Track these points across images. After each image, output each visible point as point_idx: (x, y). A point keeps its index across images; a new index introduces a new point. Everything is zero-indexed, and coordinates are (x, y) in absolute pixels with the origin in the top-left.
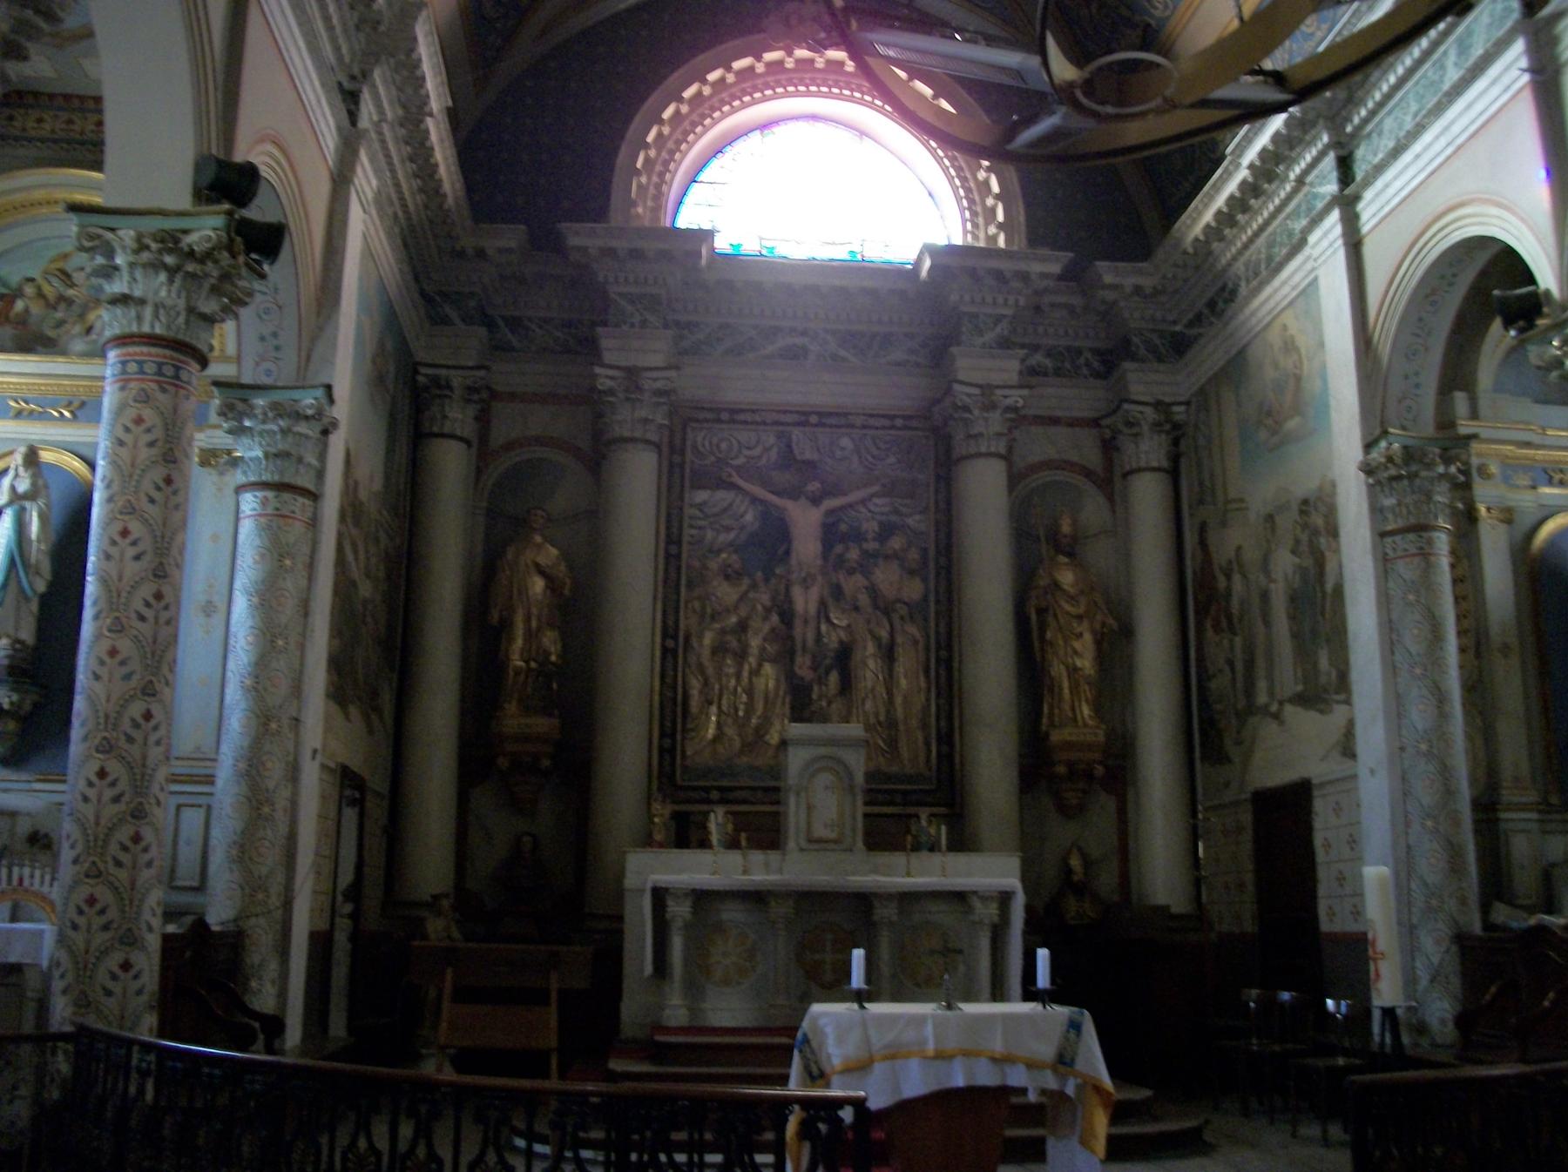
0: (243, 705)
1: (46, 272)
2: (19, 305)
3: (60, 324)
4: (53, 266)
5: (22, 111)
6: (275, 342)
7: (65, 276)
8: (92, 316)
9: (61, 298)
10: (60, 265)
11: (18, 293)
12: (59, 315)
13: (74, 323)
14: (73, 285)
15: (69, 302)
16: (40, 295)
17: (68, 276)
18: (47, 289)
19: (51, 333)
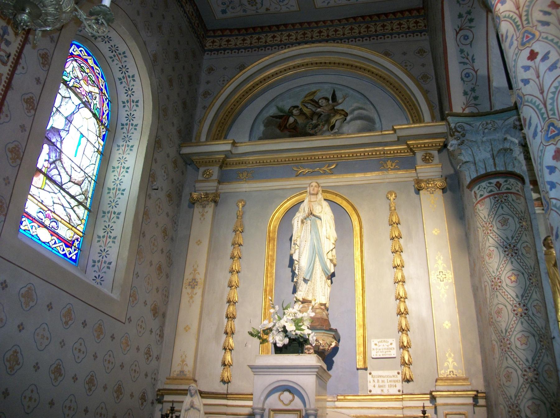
0: (519, 327)
1: (304, 103)
2: (291, 120)
3: (316, 126)
4: (307, 99)
5: (279, 33)
6: (474, 95)
7: (316, 103)
8: (333, 120)
9: (314, 113)
10: (311, 97)
11: (290, 114)
12: (314, 122)
13: (324, 125)
14: (320, 107)
15: (320, 115)
16: (302, 113)
17: (317, 103)
18: (305, 110)
19: (311, 132)
